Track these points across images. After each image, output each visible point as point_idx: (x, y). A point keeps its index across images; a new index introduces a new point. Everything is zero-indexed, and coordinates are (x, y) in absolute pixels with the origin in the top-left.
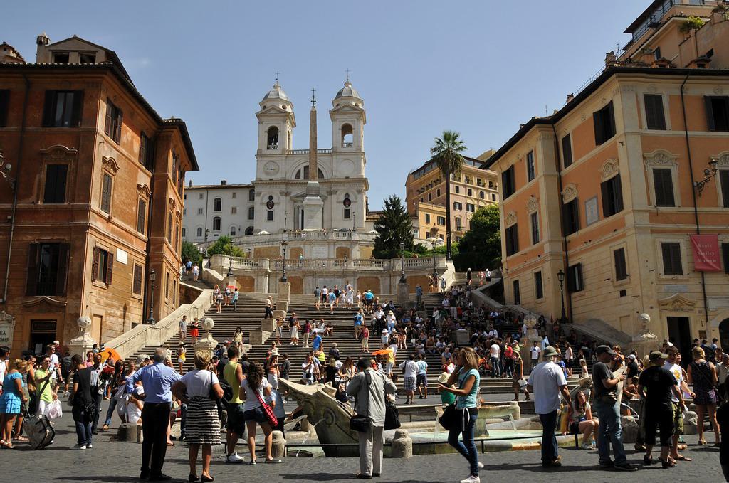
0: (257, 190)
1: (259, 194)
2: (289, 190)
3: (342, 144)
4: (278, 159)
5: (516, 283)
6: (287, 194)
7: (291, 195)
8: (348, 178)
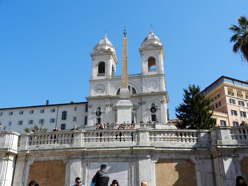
1: (91, 106)
2: (112, 103)
4: (104, 82)
8: (154, 92)
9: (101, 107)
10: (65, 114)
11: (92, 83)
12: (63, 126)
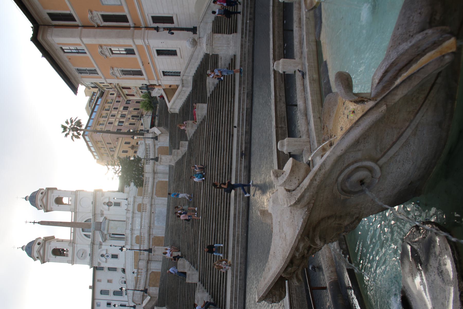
0: (96, 265)
1: (99, 263)
2: (98, 243)
3: (69, 205)
5: (165, 74)
6: (101, 244)
7: (102, 242)
8: (92, 202)
9: (101, 253)
10: (103, 292)
11: (75, 262)
12: (115, 294)
